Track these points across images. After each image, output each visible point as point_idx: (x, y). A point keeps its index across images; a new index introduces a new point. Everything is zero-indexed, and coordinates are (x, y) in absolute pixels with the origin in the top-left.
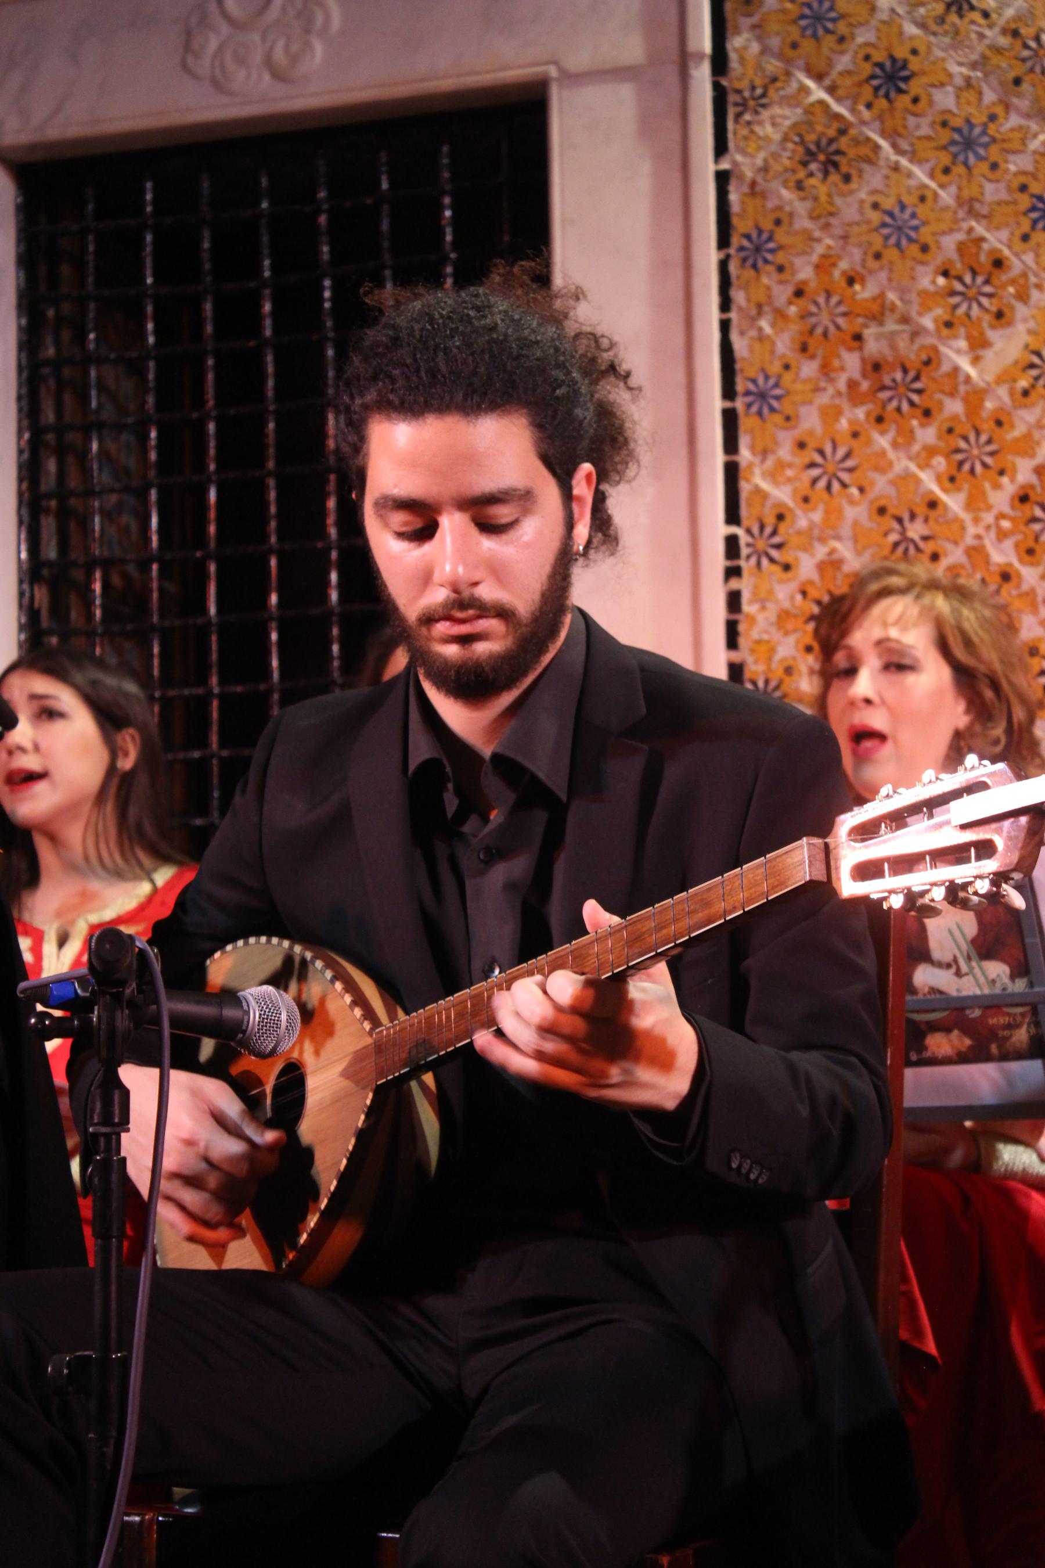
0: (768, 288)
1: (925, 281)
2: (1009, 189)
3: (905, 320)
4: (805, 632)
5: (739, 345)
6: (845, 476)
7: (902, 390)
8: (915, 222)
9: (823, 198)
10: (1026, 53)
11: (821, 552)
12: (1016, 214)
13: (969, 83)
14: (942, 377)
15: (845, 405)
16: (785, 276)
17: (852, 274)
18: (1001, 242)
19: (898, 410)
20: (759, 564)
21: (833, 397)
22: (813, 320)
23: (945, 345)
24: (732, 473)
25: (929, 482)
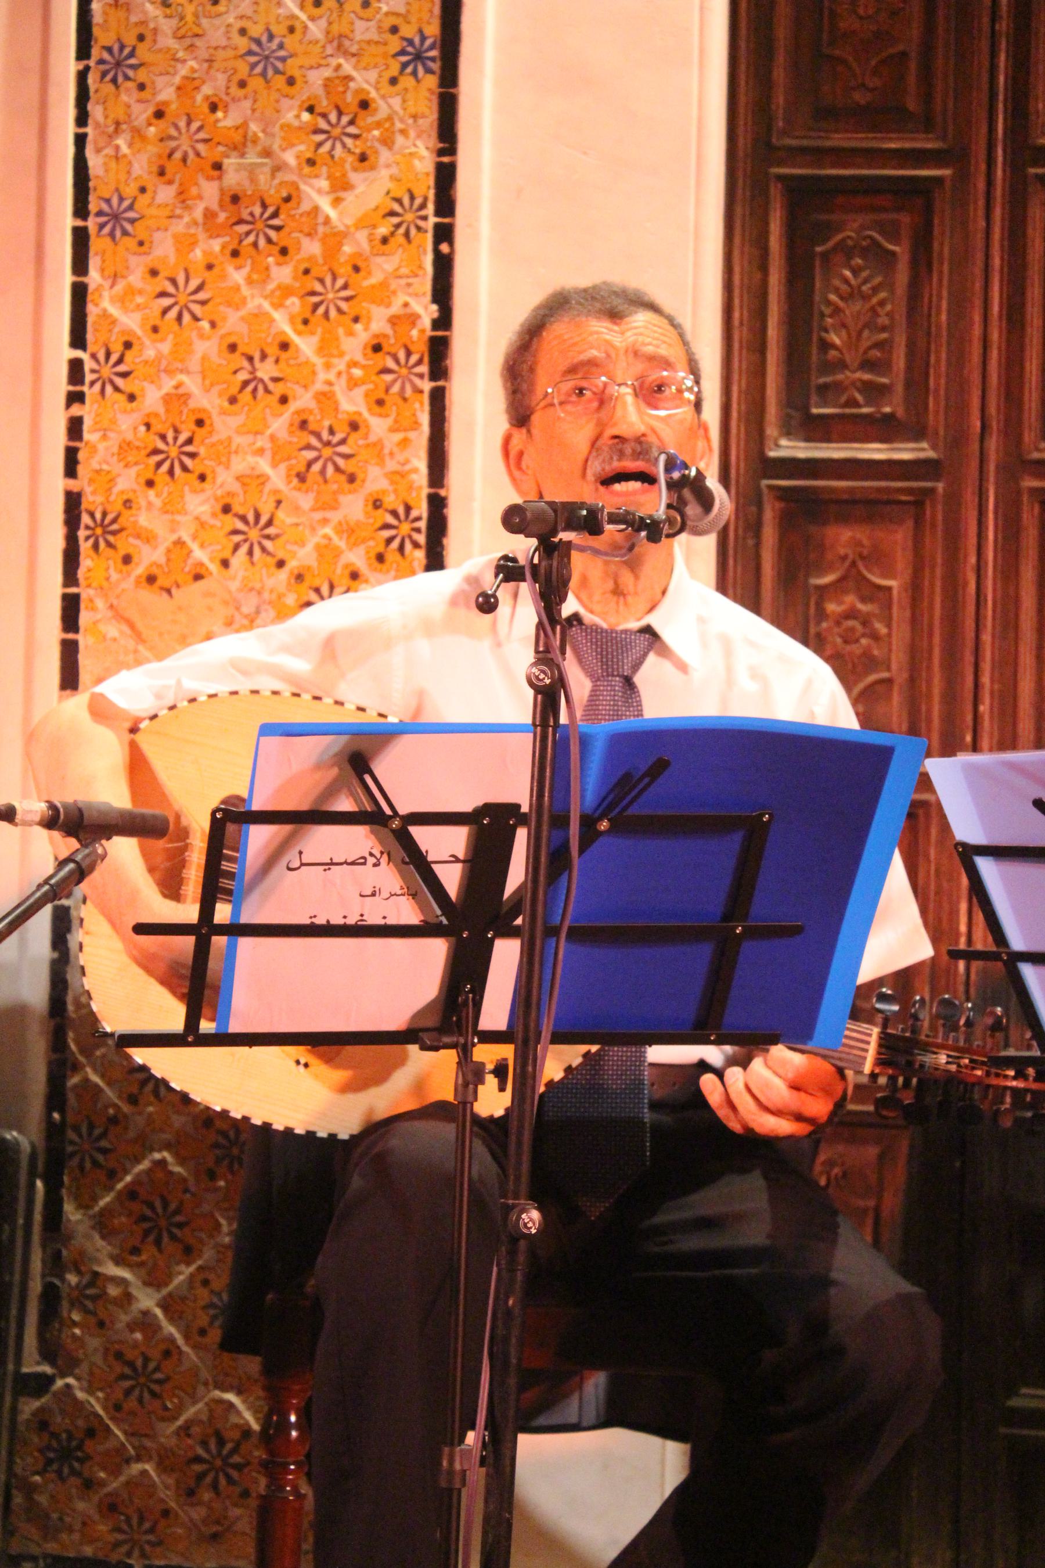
0: (129, 106)
1: (289, 117)
3: (267, 153)
4: (147, 465)
5: (94, 161)
6: (197, 309)
7: (260, 225)
8: (282, 53)
9: (189, 18)
11: (168, 385)
12: (385, 55)
14: (301, 215)
15: (200, 233)
16: (145, 95)
17: (215, 99)
18: (367, 82)
19: (255, 245)
20: (103, 391)
21: (188, 226)
22: (173, 144)
23: (306, 183)
24: (80, 294)
25: (283, 324)
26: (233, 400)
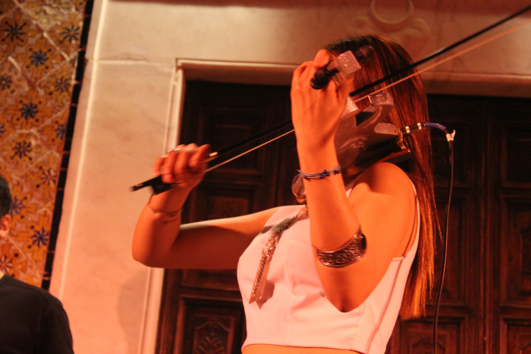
2: (27, 227)
10: (43, 176)
13: (18, 183)
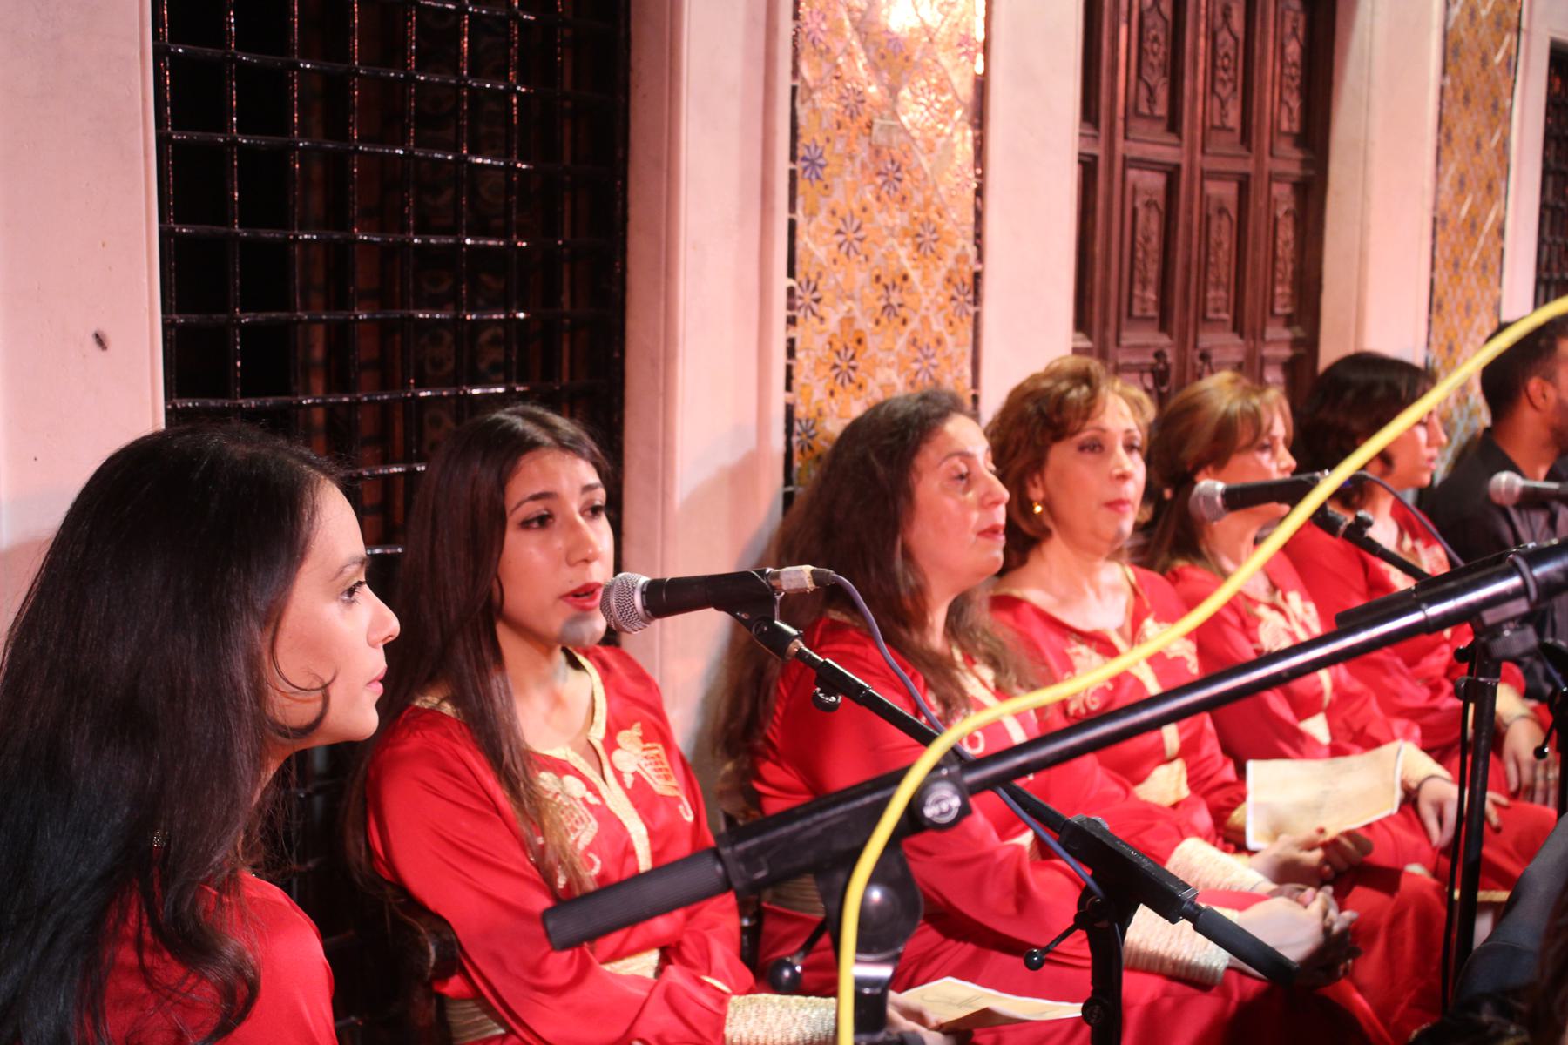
5: (802, 112)
11: (843, 308)
26: (877, 322)
